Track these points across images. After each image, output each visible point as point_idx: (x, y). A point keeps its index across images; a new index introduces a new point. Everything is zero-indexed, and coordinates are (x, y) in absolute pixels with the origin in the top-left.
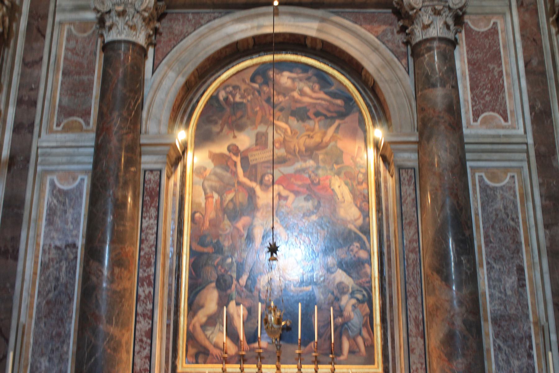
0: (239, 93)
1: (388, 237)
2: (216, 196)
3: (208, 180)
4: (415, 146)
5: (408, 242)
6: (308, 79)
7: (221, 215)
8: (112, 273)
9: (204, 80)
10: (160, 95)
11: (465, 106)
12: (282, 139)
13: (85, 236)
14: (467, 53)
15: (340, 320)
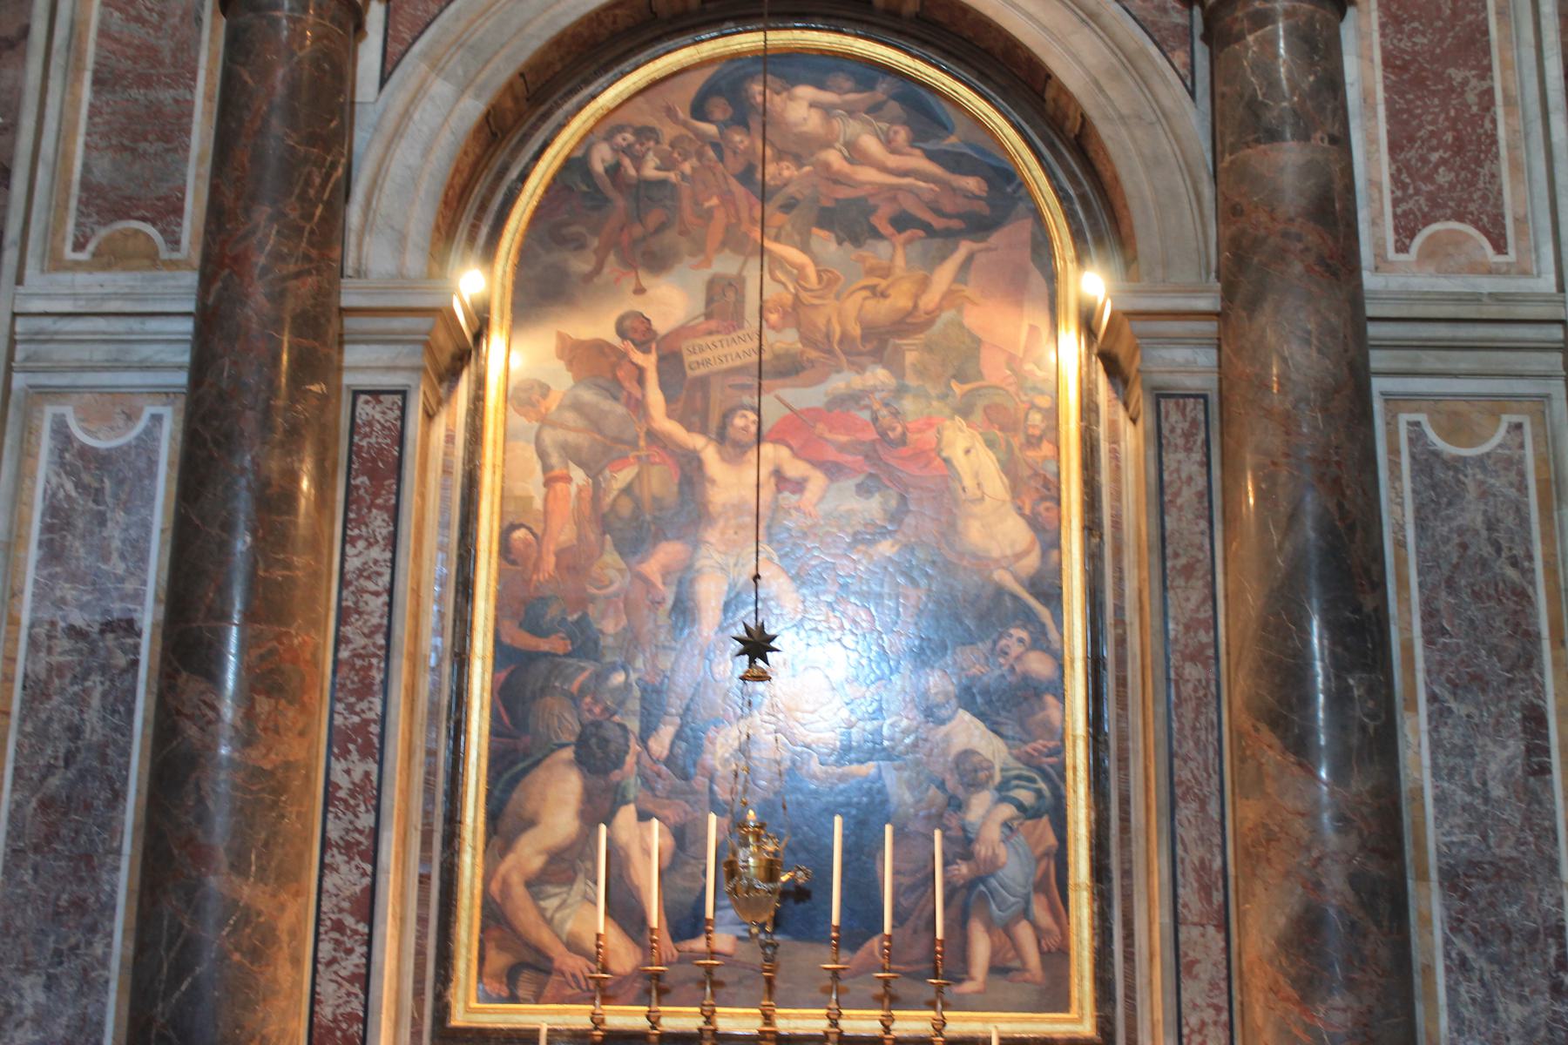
0: (656, 155)
1: (1119, 609)
2: (578, 476)
3: (554, 425)
4: (1210, 327)
5: (1181, 628)
6: (875, 109)
7: (592, 537)
8: (249, 715)
9: (543, 108)
10: (405, 155)
11: (1371, 199)
12: (788, 299)
13: (163, 596)
14: (1383, 35)
15: (963, 869)
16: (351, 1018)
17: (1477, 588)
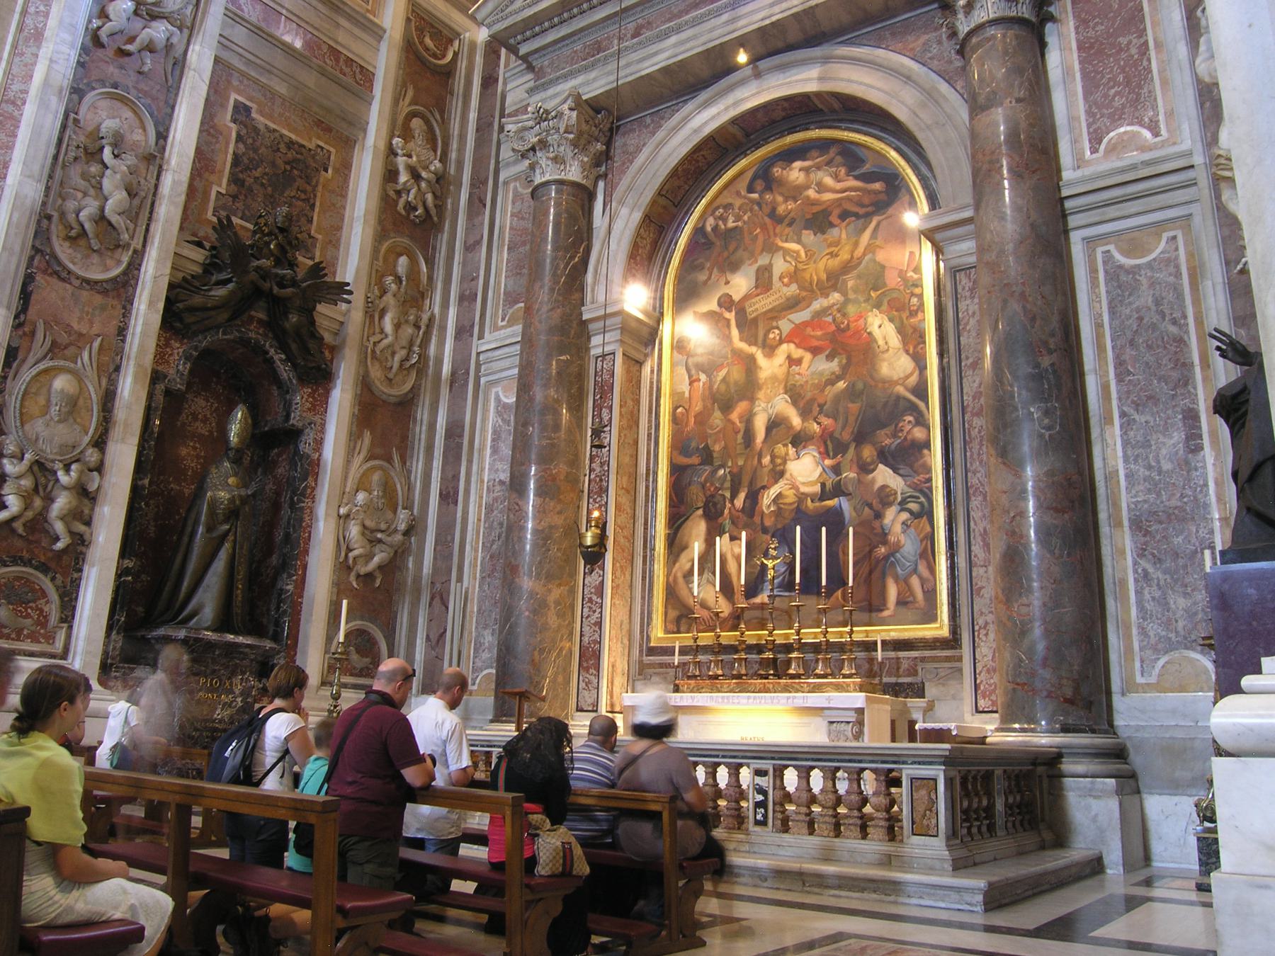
2: (703, 377)
5: (970, 398)
6: (829, 163)
14: (1077, 33)
16: (595, 642)
17: (1150, 342)
